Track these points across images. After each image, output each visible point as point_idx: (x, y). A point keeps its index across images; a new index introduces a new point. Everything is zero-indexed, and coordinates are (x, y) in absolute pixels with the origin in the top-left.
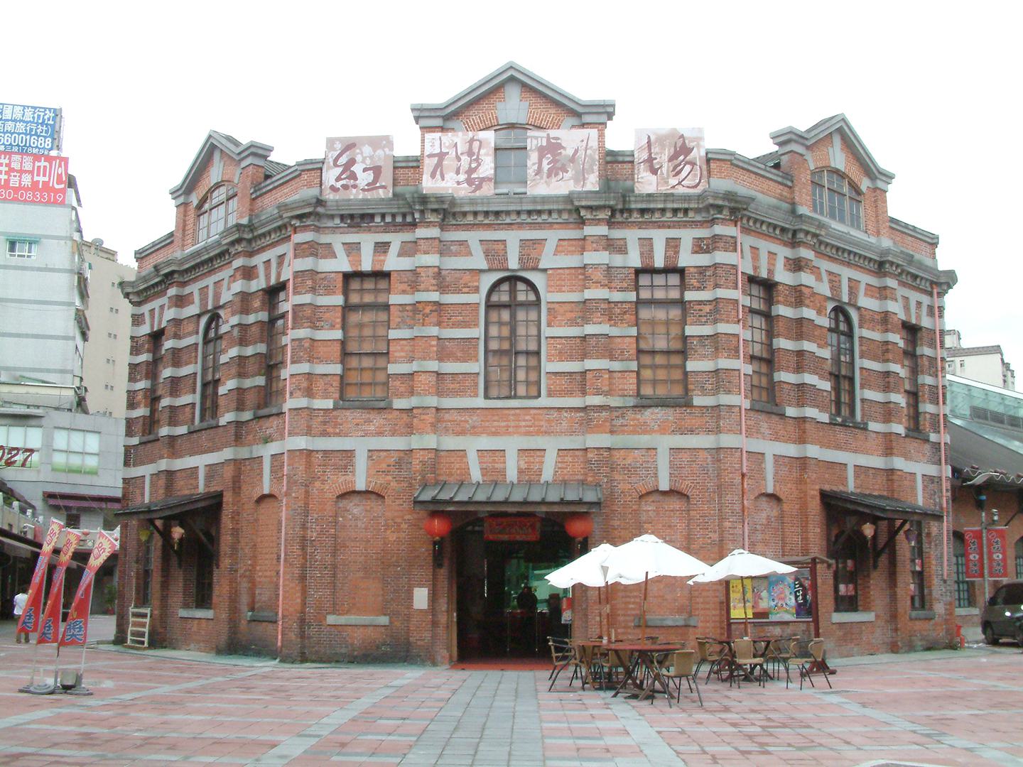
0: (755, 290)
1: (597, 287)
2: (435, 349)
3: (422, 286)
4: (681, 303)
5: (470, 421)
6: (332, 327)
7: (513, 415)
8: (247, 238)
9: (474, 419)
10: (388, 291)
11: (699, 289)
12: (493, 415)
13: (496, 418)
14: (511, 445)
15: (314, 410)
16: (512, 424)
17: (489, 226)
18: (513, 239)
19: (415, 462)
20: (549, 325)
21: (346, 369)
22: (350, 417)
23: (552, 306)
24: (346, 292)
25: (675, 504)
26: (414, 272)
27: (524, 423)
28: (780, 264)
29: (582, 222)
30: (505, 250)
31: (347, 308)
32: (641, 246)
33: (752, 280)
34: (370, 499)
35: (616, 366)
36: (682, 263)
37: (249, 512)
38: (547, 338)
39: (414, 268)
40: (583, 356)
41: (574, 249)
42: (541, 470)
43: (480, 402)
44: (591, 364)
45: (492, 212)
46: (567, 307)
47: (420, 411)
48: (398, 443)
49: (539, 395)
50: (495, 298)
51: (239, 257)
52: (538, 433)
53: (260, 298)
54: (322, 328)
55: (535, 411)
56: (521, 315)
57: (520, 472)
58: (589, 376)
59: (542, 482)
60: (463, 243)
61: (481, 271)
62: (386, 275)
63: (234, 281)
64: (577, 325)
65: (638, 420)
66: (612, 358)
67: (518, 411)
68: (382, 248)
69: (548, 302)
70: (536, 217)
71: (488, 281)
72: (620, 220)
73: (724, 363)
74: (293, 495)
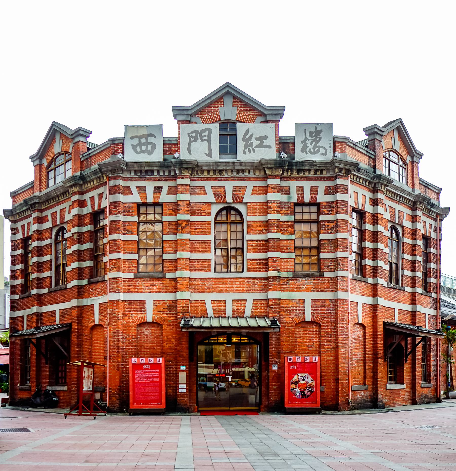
0: (354, 215)
1: (274, 213)
2: (189, 246)
3: (181, 212)
4: (317, 221)
5: (207, 285)
6: (132, 233)
7: (229, 281)
8: (81, 183)
9: (208, 284)
10: (162, 214)
11: (327, 214)
12: (219, 282)
13: (221, 283)
14: (229, 298)
15: (123, 279)
16: (229, 286)
17: (216, 179)
18: (229, 186)
19: (179, 306)
20: (248, 233)
21: (139, 256)
22: (142, 283)
23: (250, 223)
24: (139, 214)
26: (176, 204)
27: (235, 286)
28: (368, 200)
29: (266, 178)
30: (225, 192)
31: (139, 223)
32: (298, 190)
33: (354, 210)
34: (154, 326)
35: (284, 255)
36: (318, 200)
37: (87, 334)
38: (247, 240)
39: (176, 202)
40: (266, 250)
41: (261, 191)
42: (244, 311)
43: (212, 275)
44: (270, 254)
45: (218, 170)
46: (258, 224)
47: (181, 279)
48: (169, 296)
49: (242, 272)
50: (219, 218)
51: (75, 194)
52: (243, 291)
53: (89, 217)
54: (126, 234)
55: (241, 280)
56: (233, 227)
57: (234, 311)
58: (270, 261)
59: (245, 317)
60: (203, 188)
61: (211, 203)
62: (161, 205)
63: (73, 208)
64: (263, 233)
65: (295, 284)
66: (282, 252)
67: (232, 280)
68: (158, 190)
69: (248, 221)
70: (241, 174)
71: (215, 209)
72: (287, 176)
73: (340, 254)
74: (113, 324)
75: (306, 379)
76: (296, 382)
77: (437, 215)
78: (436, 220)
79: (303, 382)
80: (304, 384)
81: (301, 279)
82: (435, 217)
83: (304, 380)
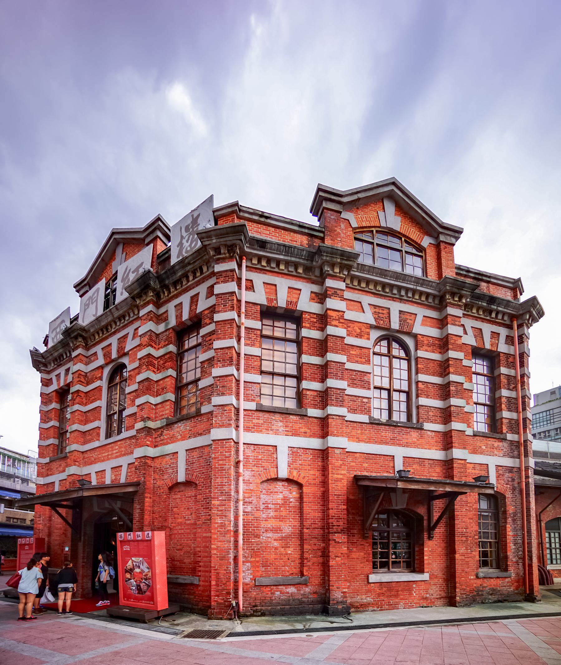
9: (94, 455)
25: (191, 492)
27: (115, 452)
75: (141, 566)
76: (131, 571)
77: (512, 317)
78: (510, 327)
79: (137, 570)
80: (140, 573)
81: (176, 425)
82: (508, 322)
83: (139, 567)
